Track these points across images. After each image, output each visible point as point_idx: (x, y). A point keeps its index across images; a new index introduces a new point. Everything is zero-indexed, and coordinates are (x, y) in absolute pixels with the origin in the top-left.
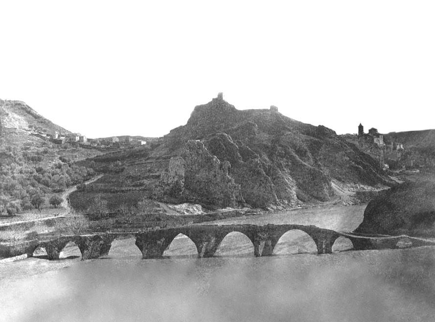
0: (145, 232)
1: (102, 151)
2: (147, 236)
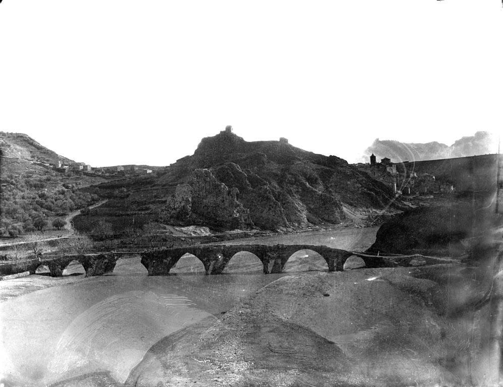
0: (151, 252)
1: (106, 179)
2: (153, 255)
